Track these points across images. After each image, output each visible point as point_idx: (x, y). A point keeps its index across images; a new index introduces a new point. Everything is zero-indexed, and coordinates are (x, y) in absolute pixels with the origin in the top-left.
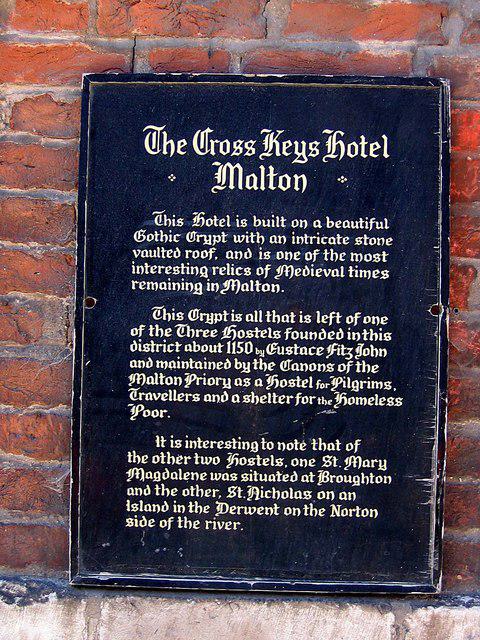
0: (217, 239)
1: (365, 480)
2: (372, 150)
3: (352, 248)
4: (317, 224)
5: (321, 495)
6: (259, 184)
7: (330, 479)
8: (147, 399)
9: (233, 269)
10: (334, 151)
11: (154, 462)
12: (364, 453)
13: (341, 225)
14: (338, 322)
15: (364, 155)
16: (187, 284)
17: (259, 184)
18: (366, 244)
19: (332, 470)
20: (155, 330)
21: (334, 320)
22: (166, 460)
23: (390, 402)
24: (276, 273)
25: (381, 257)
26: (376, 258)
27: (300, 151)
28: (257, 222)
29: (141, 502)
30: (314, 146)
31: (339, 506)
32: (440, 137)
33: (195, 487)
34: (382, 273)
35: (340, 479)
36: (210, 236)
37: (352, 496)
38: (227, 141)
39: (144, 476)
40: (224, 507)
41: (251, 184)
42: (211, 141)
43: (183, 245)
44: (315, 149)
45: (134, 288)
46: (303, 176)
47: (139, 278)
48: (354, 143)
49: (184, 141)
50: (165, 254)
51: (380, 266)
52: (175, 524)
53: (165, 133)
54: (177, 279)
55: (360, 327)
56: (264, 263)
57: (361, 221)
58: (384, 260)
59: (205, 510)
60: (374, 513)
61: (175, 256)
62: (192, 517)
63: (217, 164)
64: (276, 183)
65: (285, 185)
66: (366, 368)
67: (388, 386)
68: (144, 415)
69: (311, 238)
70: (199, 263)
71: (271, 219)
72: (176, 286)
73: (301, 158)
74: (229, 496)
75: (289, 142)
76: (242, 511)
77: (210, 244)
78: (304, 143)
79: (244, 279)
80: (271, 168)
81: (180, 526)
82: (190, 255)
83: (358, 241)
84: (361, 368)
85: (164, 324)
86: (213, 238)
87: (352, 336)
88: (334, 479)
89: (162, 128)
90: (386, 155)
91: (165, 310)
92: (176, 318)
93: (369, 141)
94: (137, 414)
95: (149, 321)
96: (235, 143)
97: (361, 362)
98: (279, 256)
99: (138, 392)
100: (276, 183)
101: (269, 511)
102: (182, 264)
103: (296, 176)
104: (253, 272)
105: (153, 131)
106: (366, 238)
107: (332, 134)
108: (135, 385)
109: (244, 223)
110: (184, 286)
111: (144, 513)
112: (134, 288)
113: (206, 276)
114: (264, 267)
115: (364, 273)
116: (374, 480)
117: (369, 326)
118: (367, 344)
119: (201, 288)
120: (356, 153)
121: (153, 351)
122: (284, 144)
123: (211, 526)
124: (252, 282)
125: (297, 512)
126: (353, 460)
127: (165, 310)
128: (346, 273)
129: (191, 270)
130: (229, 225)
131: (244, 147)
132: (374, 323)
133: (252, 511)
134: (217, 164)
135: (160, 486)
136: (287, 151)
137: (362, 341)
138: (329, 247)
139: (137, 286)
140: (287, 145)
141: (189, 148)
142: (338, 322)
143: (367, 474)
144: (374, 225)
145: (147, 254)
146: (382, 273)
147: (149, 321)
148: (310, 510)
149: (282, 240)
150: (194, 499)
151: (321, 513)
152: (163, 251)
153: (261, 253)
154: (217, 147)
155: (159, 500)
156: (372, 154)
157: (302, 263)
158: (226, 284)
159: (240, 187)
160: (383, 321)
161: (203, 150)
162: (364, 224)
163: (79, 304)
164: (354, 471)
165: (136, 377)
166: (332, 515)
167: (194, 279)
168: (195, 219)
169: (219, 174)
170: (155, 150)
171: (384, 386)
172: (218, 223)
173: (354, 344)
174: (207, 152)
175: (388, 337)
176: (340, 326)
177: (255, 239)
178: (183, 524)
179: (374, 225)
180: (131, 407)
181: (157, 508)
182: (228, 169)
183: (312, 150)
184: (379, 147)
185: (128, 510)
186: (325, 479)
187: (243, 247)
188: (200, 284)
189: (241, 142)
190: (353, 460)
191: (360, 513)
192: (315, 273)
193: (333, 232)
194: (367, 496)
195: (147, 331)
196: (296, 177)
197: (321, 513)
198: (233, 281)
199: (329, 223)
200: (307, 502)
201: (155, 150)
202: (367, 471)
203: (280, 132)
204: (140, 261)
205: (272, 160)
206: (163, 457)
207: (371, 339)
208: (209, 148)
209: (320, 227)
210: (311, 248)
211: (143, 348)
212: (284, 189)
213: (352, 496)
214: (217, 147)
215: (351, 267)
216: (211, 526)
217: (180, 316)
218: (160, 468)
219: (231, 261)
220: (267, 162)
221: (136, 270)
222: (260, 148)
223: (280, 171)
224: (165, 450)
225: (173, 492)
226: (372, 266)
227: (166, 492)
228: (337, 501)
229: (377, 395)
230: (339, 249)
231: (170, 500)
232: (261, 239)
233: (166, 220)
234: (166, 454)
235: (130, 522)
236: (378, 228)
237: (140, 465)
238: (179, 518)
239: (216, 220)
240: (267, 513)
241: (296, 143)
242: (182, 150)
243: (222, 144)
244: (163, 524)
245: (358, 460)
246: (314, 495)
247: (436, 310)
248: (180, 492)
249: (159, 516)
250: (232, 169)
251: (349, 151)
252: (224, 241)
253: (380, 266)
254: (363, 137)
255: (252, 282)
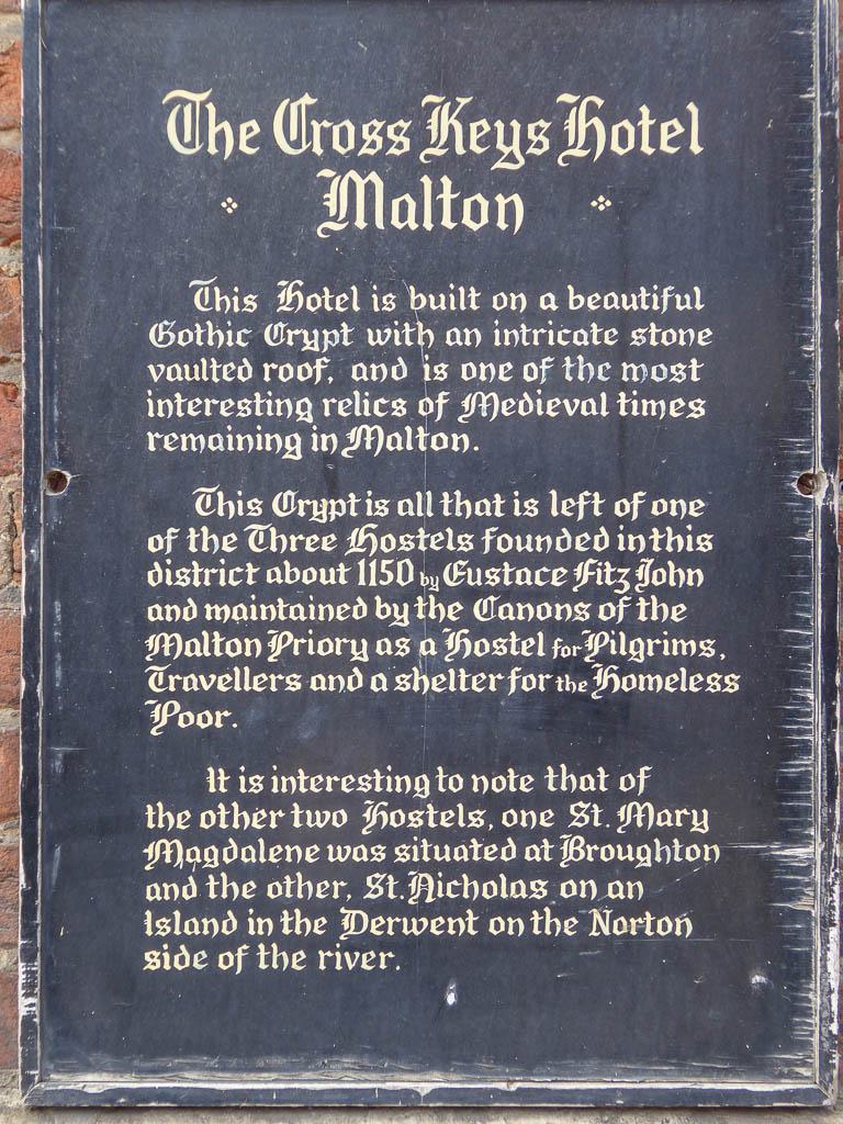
0: (332, 337)
1: (663, 854)
2: (665, 137)
3: (623, 351)
4: (547, 302)
5: (569, 890)
6: (420, 218)
7: (587, 852)
8: (186, 688)
9: (366, 402)
10: (581, 142)
11: (203, 825)
12: (657, 794)
13: (601, 302)
14: (597, 513)
15: (647, 149)
16: (268, 437)
17: (420, 218)
18: (653, 343)
19: (593, 836)
20: (200, 539)
21: (589, 508)
22: (229, 819)
23: (714, 683)
24: (462, 411)
25: (688, 371)
26: (677, 372)
27: (508, 142)
28: (418, 299)
29: (177, 914)
30: (538, 130)
31: (608, 912)
32: (817, 105)
33: (294, 878)
34: (691, 404)
35: (608, 853)
36: (316, 332)
37: (632, 890)
38: (348, 123)
39: (184, 856)
40: (359, 919)
41: (403, 217)
42: (314, 123)
43: (260, 353)
44: (541, 137)
45: (152, 448)
46: (516, 198)
47: (163, 425)
48: (626, 124)
49: (253, 124)
50: (220, 372)
51: (688, 390)
52: (252, 958)
53: (211, 107)
54: (248, 425)
55: (644, 524)
56: (433, 389)
57: (644, 293)
58: (694, 378)
59: (317, 927)
60: (680, 926)
61: (240, 376)
62: (290, 944)
63: (327, 173)
64: (457, 214)
65: (476, 217)
66: (660, 611)
67: (708, 649)
68: (181, 724)
69: (536, 332)
70: (295, 389)
71: (447, 292)
72: (245, 442)
73: (511, 158)
74: (370, 895)
75: (484, 123)
76: (398, 927)
77: (316, 349)
78: (515, 125)
79: (390, 424)
80: (446, 182)
81: (263, 966)
82: (274, 373)
83: (637, 337)
84: (649, 610)
85: (219, 525)
86: (321, 337)
87: (629, 542)
88: (596, 854)
89: (205, 96)
90: (696, 148)
91: (220, 494)
92: (246, 510)
93: (659, 116)
94: (164, 722)
95: (186, 519)
96: (365, 128)
97: (648, 600)
98: (467, 370)
99: (166, 673)
100: (457, 214)
101: (457, 927)
102: (257, 395)
103: (500, 199)
104: (412, 408)
105: (184, 102)
106: (654, 329)
107: (578, 104)
108: (160, 659)
109: (389, 303)
110: (264, 442)
111: (184, 939)
112: (152, 448)
113: (310, 420)
114: (434, 399)
115: (649, 407)
116: (682, 854)
117: (664, 521)
118: (661, 560)
119: (298, 447)
120: (631, 145)
121: (197, 583)
122: (473, 126)
123: (330, 962)
124: (409, 429)
125: (516, 926)
126: (634, 810)
127: (220, 494)
128: (613, 406)
129: (277, 407)
130: (356, 308)
131: (386, 136)
132: (674, 513)
133: (420, 926)
134: (327, 173)
135: (218, 878)
136: (479, 143)
137: (649, 553)
138: (573, 351)
139: (159, 442)
140: (480, 129)
141: (265, 140)
142: (597, 513)
143: (667, 841)
144: (672, 301)
145: (178, 373)
146: (691, 404)
147: (186, 519)
148: (545, 923)
149: (473, 337)
150: (291, 905)
151: (568, 927)
152: (215, 366)
153: (427, 367)
154: (326, 135)
155: (218, 909)
156: (664, 147)
157: (515, 388)
158: (354, 435)
159: (380, 224)
160: (694, 508)
161: (296, 144)
162: (649, 301)
163: (31, 490)
164: (637, 836)
165: (162, 641)
166: (594, 933)
167: (285, 426)
168: (281, 296)
169: (332, 195)
170: (191, 145)
171: (699, 650)
172: (333, 303)
173: (629, 560)
174: (305, 147)
175: (705, 544)
176: (602, 521)
177: (414, 337)
178: (269, 960)
179: (672, 301)
180: (153, 707)
181: (211, 927)
182: (352, 185)
183: (535, 139)
184: (680, 130)
185: (149, 932)
186: (576, 854)
187: (387, 355)
188: (296, 436)
189: (379, 125)
190: (634, 810)
191: (654, 928)
192: (544, 408)
193: (580, 319)
194: (668, 890)
195: (182, 542)
196: (501, 200)
197: (568, 927)
198: (369, 430)
199: (576, 301)
200: (540, 906)
201: (191, 145)
202: (666, 835)
203: (463, 101)
204: (165, 390)
205: (448, 164)
206: (223, 813)
207: (669, 549)
208: (310, 137)
209: (554, 307)
210: (535, 354)
211: (174, 579)
212: (475, 227)
213: (636, 889)
214: (326, 135)
215: (622, 395)
216: (330, 962)
217: (255, 506)
218: (217, 837)
219: (363, 386)
220: (437, 168)
221: (156, 408)
222: (420, 137)
223: (463, 188)
224: (227, 800)
225: (246, 892)
226: (666, 391)
227: (230, 890)
228: (603, 902)
229: (683, 670)
230: (595, 354)
231: (240, 907)
232: (426, 338)
233: (218, 299)
234: (229, 808)
235: (152, 961)
236: (679, 307)
237: (171, 834)
238: (261, 947)
239: (327, 296)
240: (451, 931)
241: (499, 125)
242: (250, 143)
243: (336, 130)
244: (226, 961)
245: (646, 811)
246: (553, 890)
247: (804, 482)
248: (262, 888)
249: (216, 945)
250: (360, 184)
251: (616, 139)
252: (346, 343)
253: (688, 390)
254: (645, 110)
255: (409, 429)
